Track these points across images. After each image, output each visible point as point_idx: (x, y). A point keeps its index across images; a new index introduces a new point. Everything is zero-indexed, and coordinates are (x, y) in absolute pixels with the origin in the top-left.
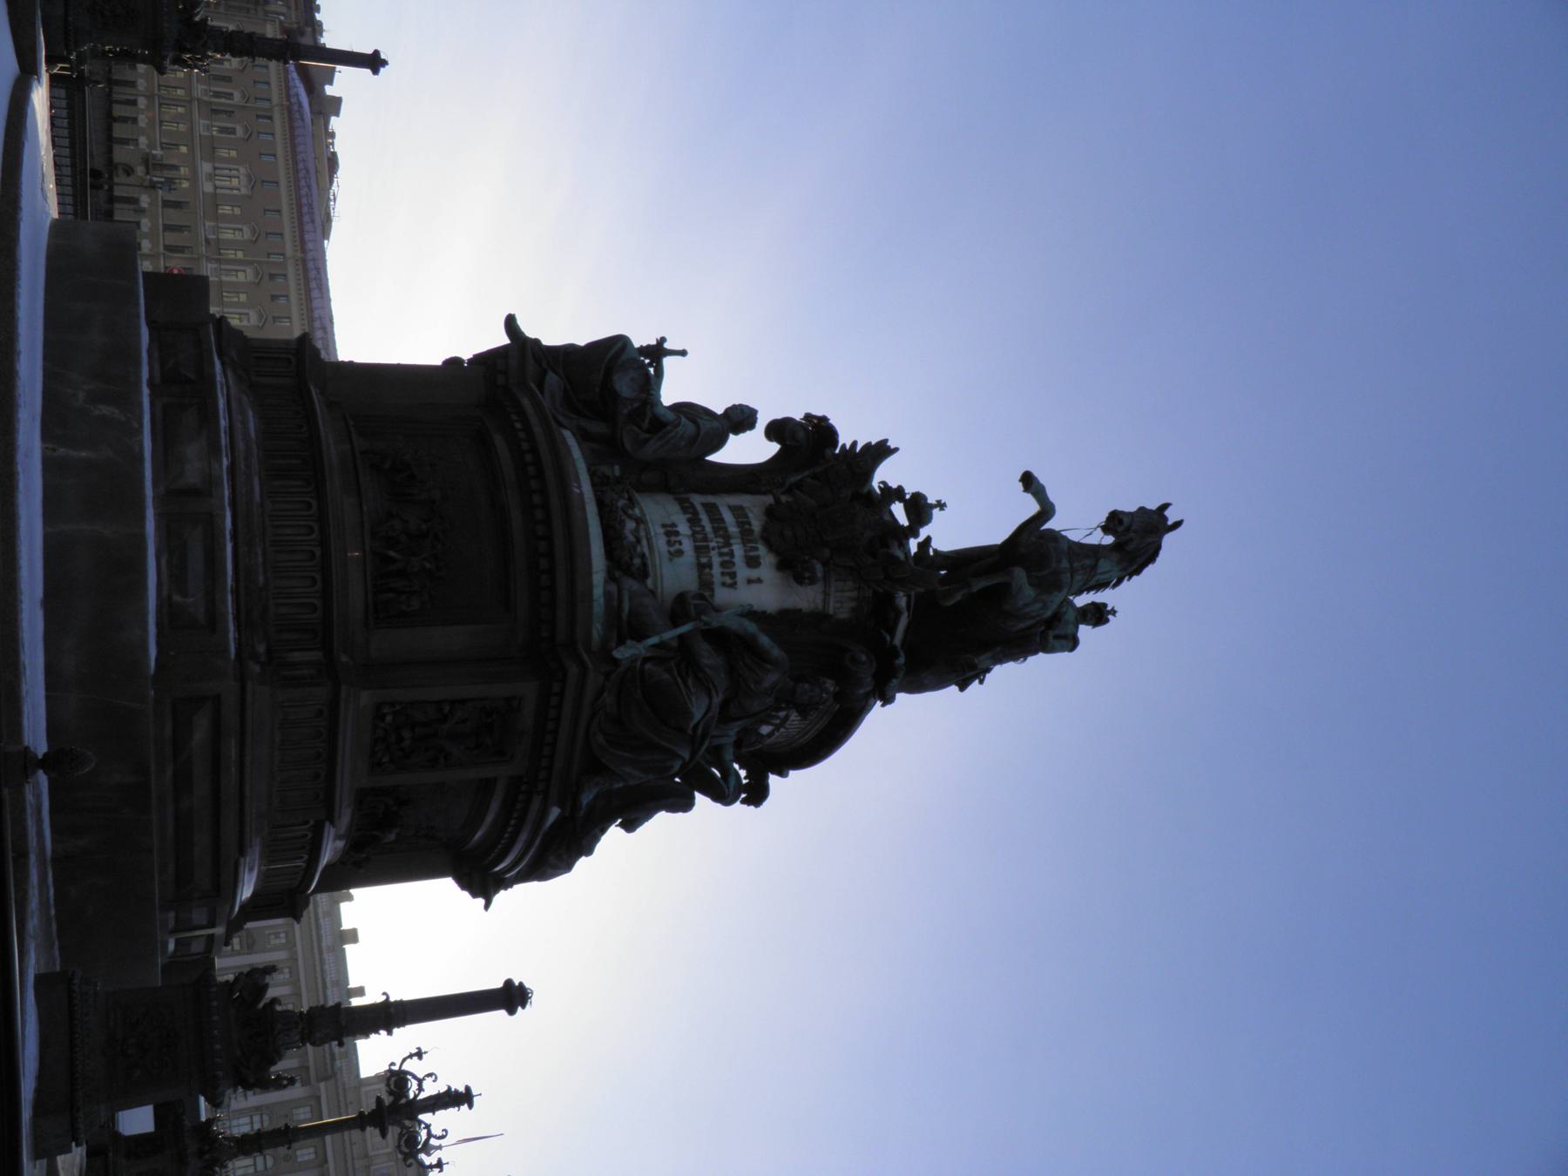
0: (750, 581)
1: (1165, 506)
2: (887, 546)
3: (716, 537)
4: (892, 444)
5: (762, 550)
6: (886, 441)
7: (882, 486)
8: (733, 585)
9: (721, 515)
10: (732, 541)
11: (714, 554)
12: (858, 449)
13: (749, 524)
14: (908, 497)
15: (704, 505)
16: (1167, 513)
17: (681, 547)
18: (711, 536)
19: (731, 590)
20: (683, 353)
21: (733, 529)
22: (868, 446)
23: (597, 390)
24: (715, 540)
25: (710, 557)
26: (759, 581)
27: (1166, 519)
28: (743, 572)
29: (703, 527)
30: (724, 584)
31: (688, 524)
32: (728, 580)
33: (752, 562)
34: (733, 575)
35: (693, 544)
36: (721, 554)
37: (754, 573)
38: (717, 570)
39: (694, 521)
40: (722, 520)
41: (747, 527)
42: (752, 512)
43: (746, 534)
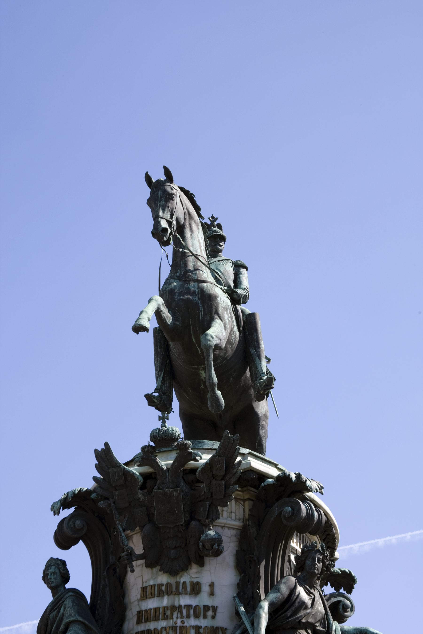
0: (212, 594)
1: (148, 178)
2: (194, 470)
3: (173, 619)
4: (101, 447)
6: (96, 450)
8: (215, 609)
10: (177, 604)
11: (186, 624)
12: (99, 476)
13: (160, 585)
14: (152, 444)
15: (139, 622)
18: (171, 623)
19: (219, 611)
21: (165, 602)
22: (98, 467)
24: (175, 619)
25: (190, 626)
26: (212, 585)
30: (213, 617)
32: (210, 613)
34: (206, 608)
36: (188, 617)
37: (205, 589)
40: (156, 610)
41: (163, 588)
42: (148, 580)
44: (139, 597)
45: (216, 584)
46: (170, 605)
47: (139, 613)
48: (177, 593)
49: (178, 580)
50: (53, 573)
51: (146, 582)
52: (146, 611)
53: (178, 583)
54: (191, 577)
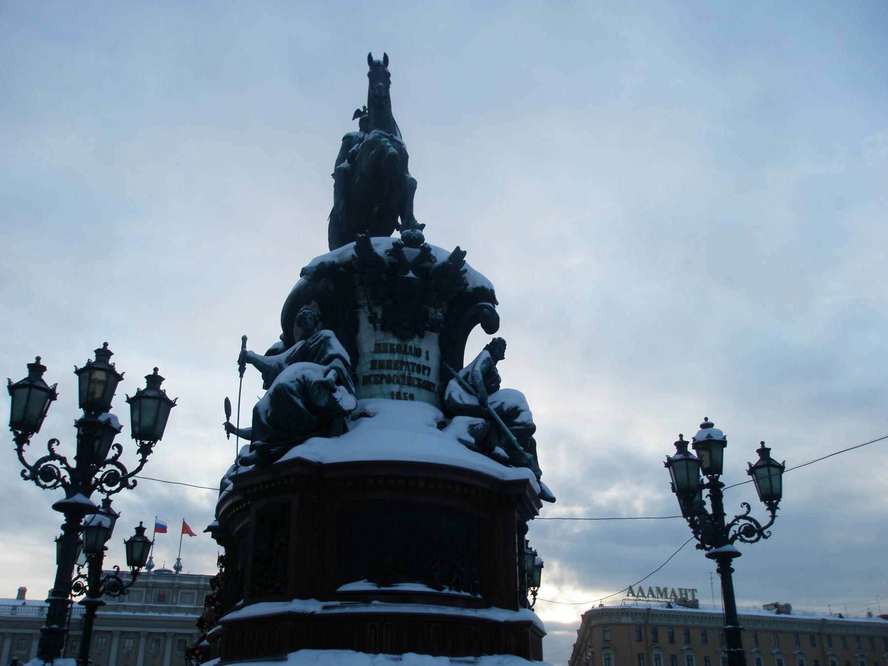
0: (427, 358)
1: (370, 57)
3: (402, 370)
5: (410, 343)
7: (388, 253)
8: (429, 369)
9: (384, 360)
10: (405, 360)
11: (412, 375)
13: (392, 345)
16: (374, 59)
17: (409, 393)
18: (401, 373)
20: (244, 339)
21: (396, 357)
23: (315, 417)
25: (415, 378)
26: (427, 353)
27: (379, 63)
28: (422, 361)
29: (395, 375)
30: (428, 375)
31: (392, 384)
32: (426, 372)
33: (418, 353)
34: (425, 368)
35: (406, 386)
36: (413, 371)
37: (424, 354)
38: (421, 376)
39: (390, 380)
40: (389, 361)
41: (395, 347)
43: (400, 350)
44: (373, 349)
45: (429, 353)
46: (400, 360)
47: (373, 362)
48: (405, 353)
49: (406, 344)
50: (310, 318)
51: (379, 340)
52: (380, 361)
53: (406, 346)
54: (415, 344)
